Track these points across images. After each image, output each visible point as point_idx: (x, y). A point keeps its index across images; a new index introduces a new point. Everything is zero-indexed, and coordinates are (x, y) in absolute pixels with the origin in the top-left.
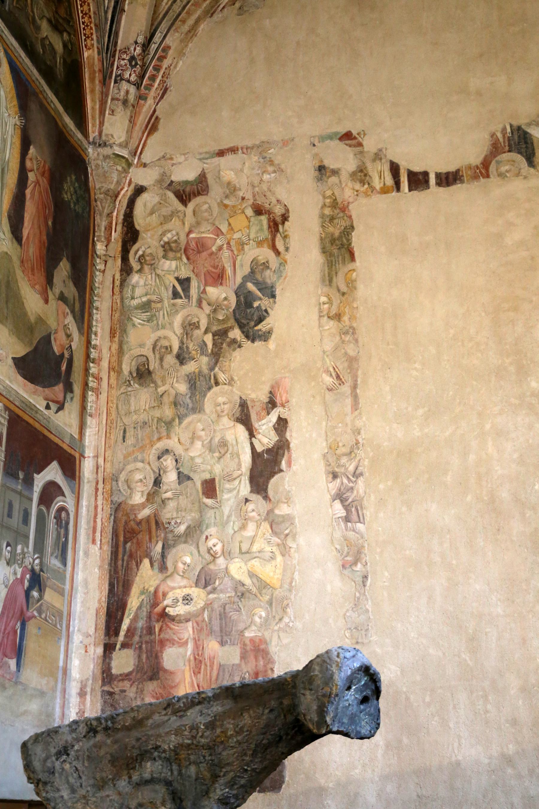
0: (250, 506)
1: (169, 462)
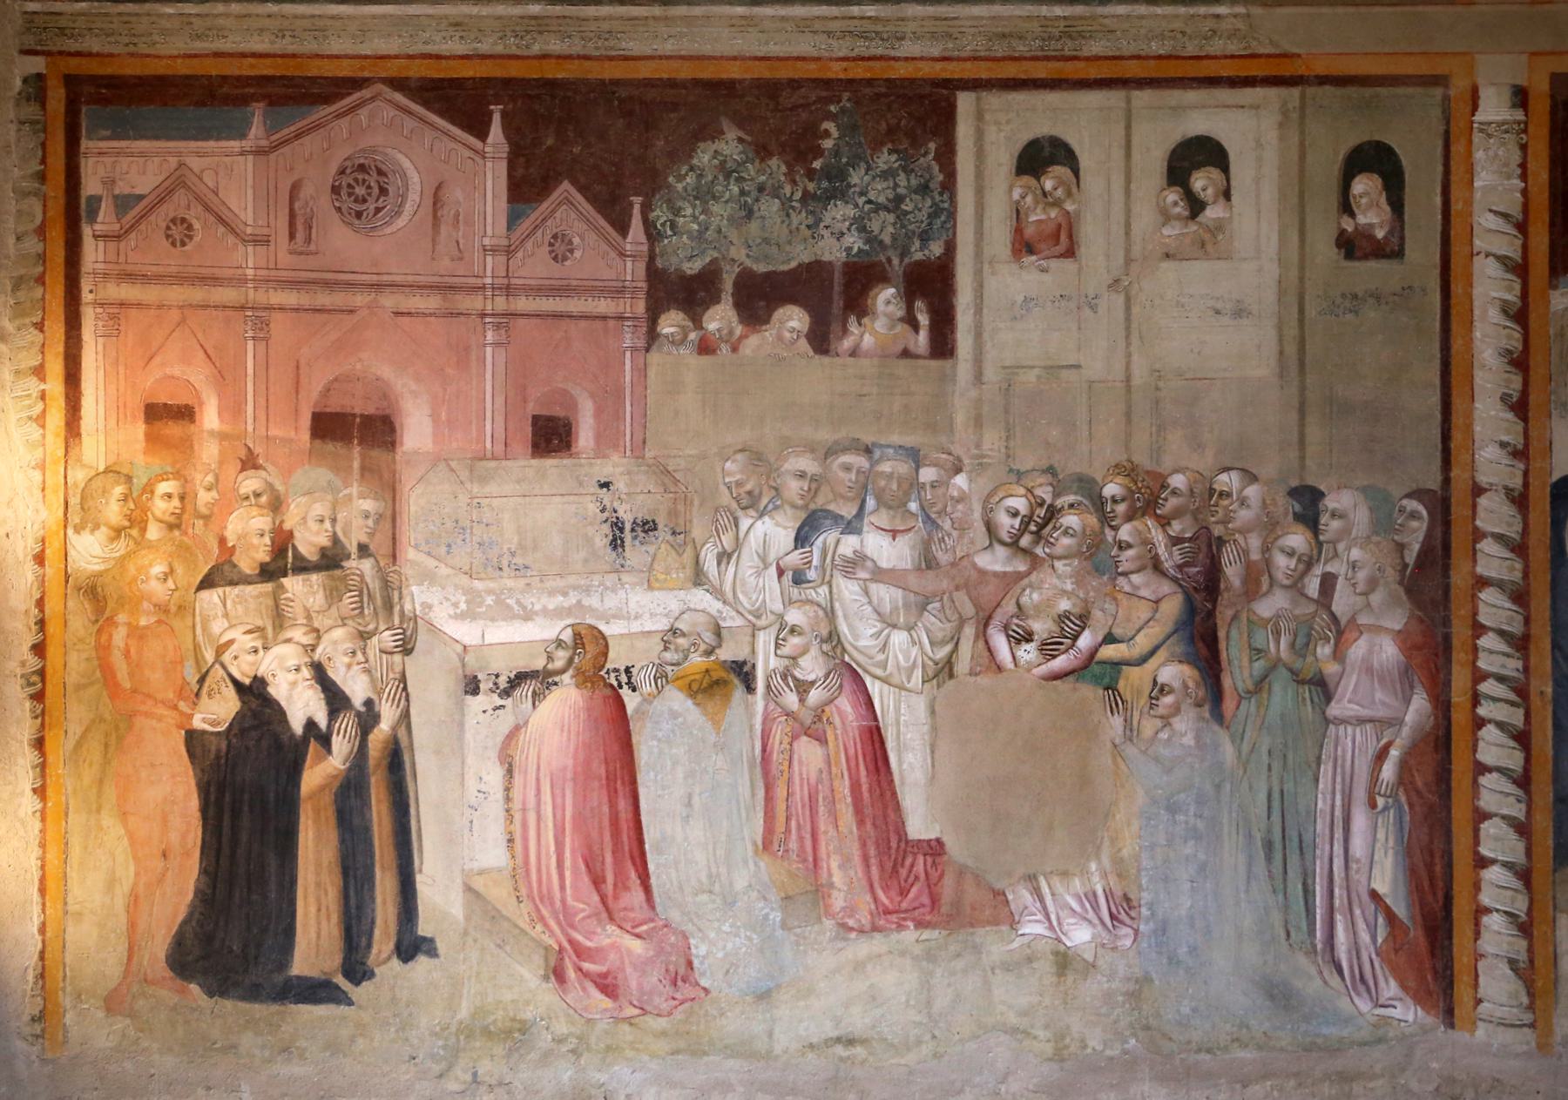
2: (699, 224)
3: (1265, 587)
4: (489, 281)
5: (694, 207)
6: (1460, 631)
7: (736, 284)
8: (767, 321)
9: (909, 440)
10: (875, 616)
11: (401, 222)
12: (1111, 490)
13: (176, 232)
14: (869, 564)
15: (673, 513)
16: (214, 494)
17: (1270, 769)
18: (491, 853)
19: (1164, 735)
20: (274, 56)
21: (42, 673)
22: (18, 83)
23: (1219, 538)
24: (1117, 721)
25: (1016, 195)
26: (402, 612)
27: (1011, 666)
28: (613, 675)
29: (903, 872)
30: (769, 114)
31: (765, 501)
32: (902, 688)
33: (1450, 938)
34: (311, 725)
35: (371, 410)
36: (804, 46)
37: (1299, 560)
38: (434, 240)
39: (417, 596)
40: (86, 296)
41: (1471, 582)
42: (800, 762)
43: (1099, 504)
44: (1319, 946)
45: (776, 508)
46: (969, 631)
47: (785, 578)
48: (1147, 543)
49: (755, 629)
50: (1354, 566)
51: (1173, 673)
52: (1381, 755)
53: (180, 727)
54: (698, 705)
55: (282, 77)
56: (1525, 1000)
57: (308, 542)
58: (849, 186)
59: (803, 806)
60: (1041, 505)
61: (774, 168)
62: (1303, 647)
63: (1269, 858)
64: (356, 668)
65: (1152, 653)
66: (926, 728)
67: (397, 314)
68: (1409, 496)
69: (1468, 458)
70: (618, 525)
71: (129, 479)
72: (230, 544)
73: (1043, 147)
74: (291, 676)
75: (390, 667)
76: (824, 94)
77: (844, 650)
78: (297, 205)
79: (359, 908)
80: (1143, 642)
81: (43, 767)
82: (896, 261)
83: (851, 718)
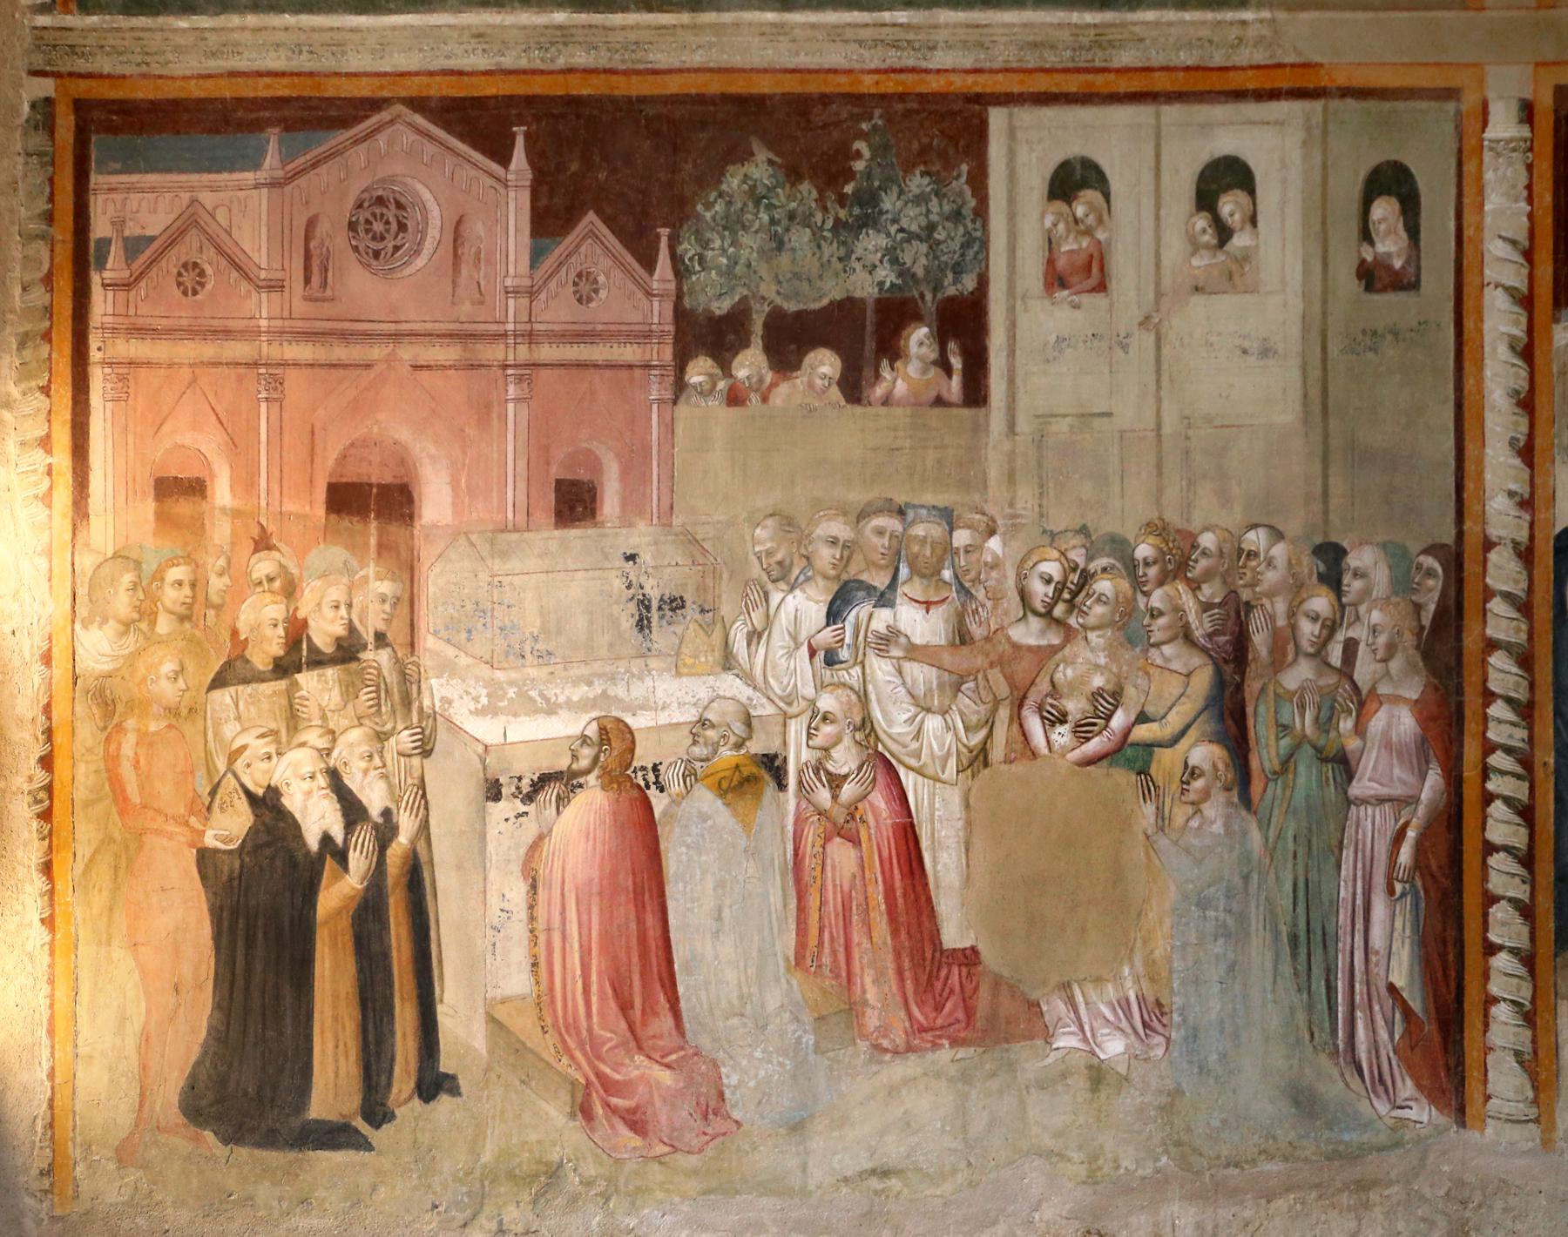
2: (728, 258)
3: (1290, 657)
4: (510, 327)
5: (723, 238)
6: (1472, 699)
7: (767, 326)
8: (797, 366)
9: (942, 500)
10: (908, 699)
11: (420, 262)
12: (1144, 551)
13: (189, 279)
14: (902, 640)
15: (701, 589)
17: (1295, 857)
18: (517, 981)
19: (1194, 823)
20: (292, 74)
21: (49, 788)
23: (1247, 603)
24: (1149, 809)
25: (1048, 222)
26: (421, 709)
27: (1045, 751)
28: (640, 774)
29: (938, 985)
30: (799, 133)
31: (796, 571)
32: (937, 780)
33: (1462, 1031)
35: (388, 479)
36: (835, 57)
37: (1323, 626)
38: (454, 282)
39: (437, 690)
40: (95, 355)
41: (1482, 645)
42: (833, 867)
43: (1131, 566)
44: (1341, 1046)
45: (808, 579)
46: (1004, 713)
47: (817, 659)
48: (1178, 610)
49: (786, 717)
50: (1374, 630)
51: (1205, 754)
52: (1399, 837)
53: (192, 845)
54: (727, 805)
55: (298, 98)
56: (1530, 1094)
57: (324, 631)
58: (881, 213)
59: (837, 916)
60: (1074, 570)
61: (805, 194)
62: (1326, 723)
63: (1294, 955)
64: (373, 773)
65: (1183, 733)
66: (960, 824)
67: (416, 367)
68: (1426, 551)
69: (1479, 508)
70: (644, 604)
71: (138, 564)
72: (243, 637)
73: (1074, 169)
75: (409, 772)
76: (856, 110)
77: (878, 738)
78: (312, 244)
79: (378, 1043)
80: (1175, 721)
81: (51, 893)
82: (929, 297)
83: (884, 814)
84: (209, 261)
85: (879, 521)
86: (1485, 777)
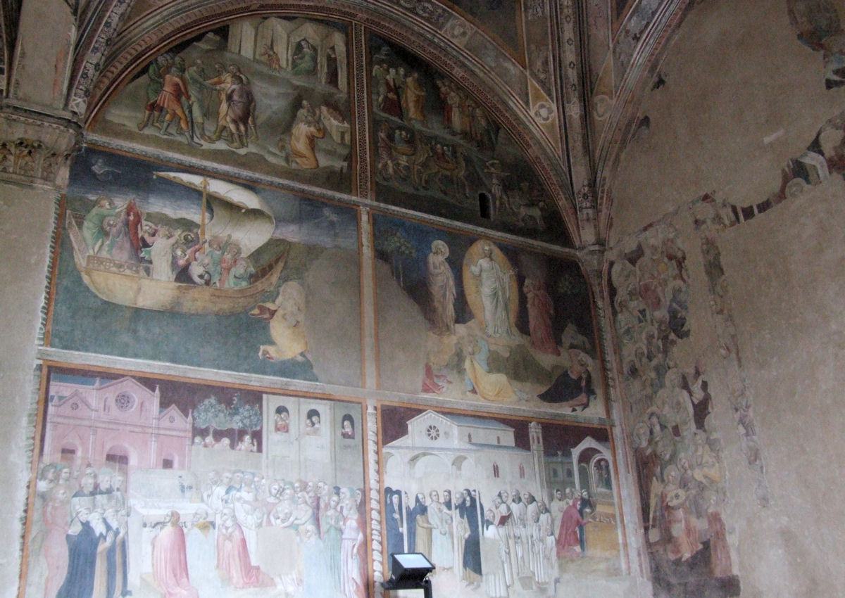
0: (698, 437)
1: (654, 420)
6: (368, 520)
8: (220, 441)
9: (252, 471)
11: (133, 409)
12: (297, 485)
16: (79, 473)
19: (308, 542)
22: (35, 366)
32: (250, 529)
34: (101, 534)
35: (122, 454)
43: (293, 488)
46: (265, 516)
48: (304, 497)
49: (216, 514)
50: (347, 505)
57: (104, 486)
74: (97, 521)
80: (304, 520)
84: (79, 403)
85: (238, 474)
86: (372, 535)
